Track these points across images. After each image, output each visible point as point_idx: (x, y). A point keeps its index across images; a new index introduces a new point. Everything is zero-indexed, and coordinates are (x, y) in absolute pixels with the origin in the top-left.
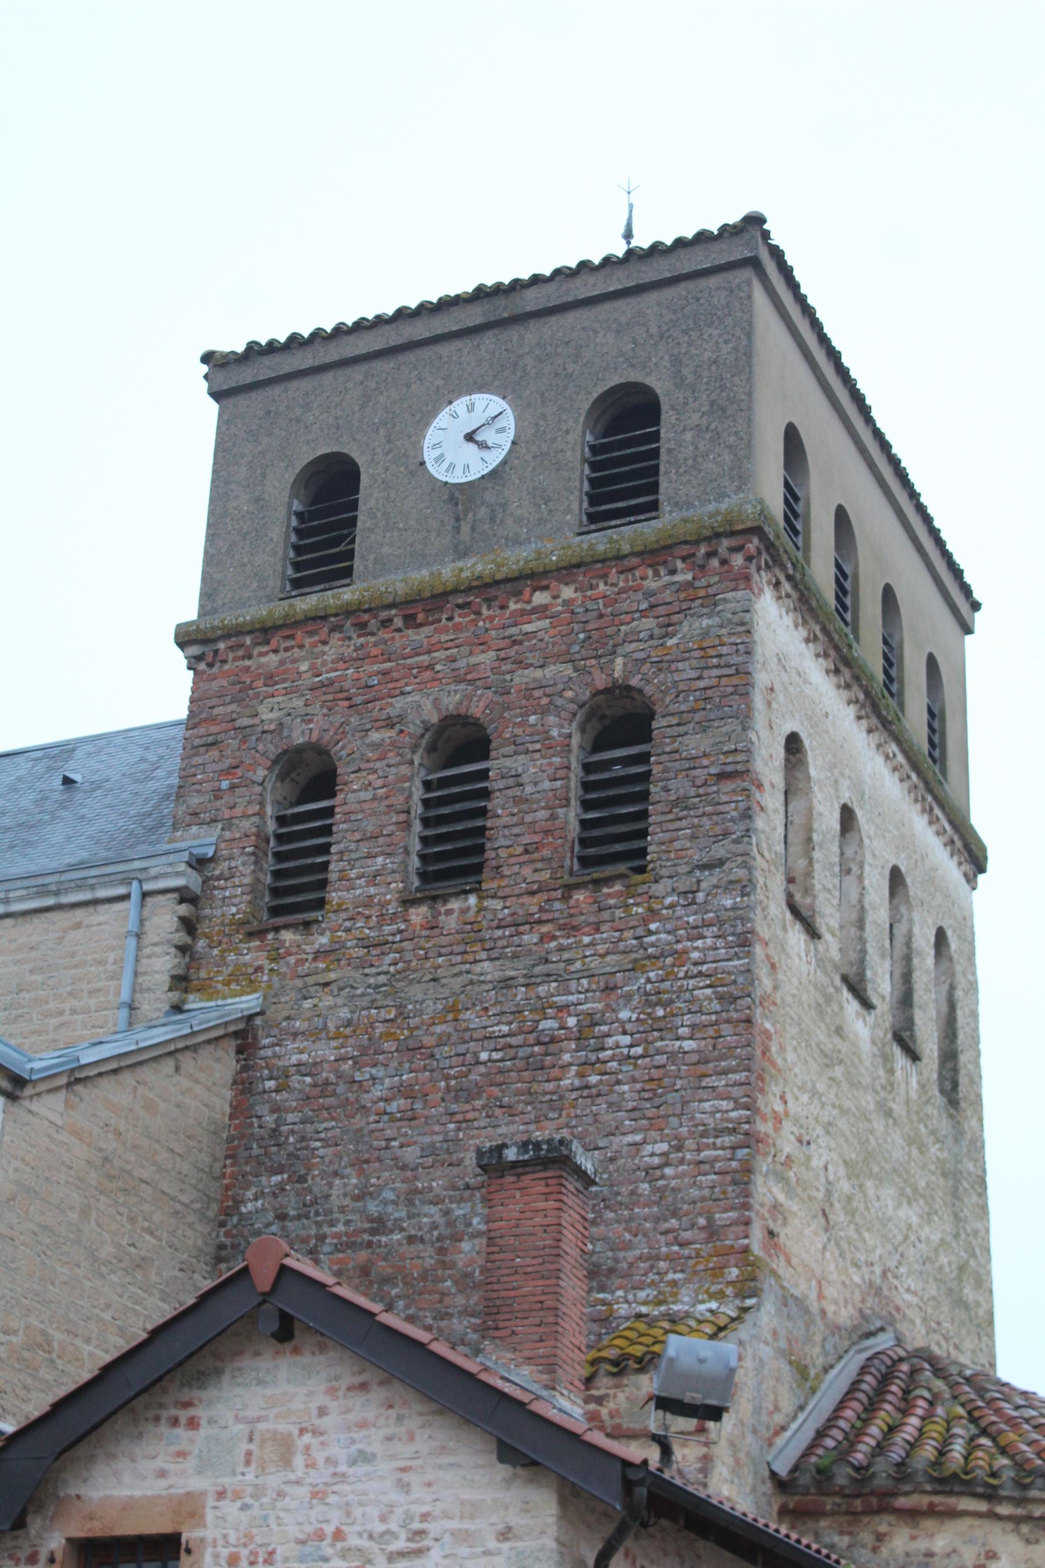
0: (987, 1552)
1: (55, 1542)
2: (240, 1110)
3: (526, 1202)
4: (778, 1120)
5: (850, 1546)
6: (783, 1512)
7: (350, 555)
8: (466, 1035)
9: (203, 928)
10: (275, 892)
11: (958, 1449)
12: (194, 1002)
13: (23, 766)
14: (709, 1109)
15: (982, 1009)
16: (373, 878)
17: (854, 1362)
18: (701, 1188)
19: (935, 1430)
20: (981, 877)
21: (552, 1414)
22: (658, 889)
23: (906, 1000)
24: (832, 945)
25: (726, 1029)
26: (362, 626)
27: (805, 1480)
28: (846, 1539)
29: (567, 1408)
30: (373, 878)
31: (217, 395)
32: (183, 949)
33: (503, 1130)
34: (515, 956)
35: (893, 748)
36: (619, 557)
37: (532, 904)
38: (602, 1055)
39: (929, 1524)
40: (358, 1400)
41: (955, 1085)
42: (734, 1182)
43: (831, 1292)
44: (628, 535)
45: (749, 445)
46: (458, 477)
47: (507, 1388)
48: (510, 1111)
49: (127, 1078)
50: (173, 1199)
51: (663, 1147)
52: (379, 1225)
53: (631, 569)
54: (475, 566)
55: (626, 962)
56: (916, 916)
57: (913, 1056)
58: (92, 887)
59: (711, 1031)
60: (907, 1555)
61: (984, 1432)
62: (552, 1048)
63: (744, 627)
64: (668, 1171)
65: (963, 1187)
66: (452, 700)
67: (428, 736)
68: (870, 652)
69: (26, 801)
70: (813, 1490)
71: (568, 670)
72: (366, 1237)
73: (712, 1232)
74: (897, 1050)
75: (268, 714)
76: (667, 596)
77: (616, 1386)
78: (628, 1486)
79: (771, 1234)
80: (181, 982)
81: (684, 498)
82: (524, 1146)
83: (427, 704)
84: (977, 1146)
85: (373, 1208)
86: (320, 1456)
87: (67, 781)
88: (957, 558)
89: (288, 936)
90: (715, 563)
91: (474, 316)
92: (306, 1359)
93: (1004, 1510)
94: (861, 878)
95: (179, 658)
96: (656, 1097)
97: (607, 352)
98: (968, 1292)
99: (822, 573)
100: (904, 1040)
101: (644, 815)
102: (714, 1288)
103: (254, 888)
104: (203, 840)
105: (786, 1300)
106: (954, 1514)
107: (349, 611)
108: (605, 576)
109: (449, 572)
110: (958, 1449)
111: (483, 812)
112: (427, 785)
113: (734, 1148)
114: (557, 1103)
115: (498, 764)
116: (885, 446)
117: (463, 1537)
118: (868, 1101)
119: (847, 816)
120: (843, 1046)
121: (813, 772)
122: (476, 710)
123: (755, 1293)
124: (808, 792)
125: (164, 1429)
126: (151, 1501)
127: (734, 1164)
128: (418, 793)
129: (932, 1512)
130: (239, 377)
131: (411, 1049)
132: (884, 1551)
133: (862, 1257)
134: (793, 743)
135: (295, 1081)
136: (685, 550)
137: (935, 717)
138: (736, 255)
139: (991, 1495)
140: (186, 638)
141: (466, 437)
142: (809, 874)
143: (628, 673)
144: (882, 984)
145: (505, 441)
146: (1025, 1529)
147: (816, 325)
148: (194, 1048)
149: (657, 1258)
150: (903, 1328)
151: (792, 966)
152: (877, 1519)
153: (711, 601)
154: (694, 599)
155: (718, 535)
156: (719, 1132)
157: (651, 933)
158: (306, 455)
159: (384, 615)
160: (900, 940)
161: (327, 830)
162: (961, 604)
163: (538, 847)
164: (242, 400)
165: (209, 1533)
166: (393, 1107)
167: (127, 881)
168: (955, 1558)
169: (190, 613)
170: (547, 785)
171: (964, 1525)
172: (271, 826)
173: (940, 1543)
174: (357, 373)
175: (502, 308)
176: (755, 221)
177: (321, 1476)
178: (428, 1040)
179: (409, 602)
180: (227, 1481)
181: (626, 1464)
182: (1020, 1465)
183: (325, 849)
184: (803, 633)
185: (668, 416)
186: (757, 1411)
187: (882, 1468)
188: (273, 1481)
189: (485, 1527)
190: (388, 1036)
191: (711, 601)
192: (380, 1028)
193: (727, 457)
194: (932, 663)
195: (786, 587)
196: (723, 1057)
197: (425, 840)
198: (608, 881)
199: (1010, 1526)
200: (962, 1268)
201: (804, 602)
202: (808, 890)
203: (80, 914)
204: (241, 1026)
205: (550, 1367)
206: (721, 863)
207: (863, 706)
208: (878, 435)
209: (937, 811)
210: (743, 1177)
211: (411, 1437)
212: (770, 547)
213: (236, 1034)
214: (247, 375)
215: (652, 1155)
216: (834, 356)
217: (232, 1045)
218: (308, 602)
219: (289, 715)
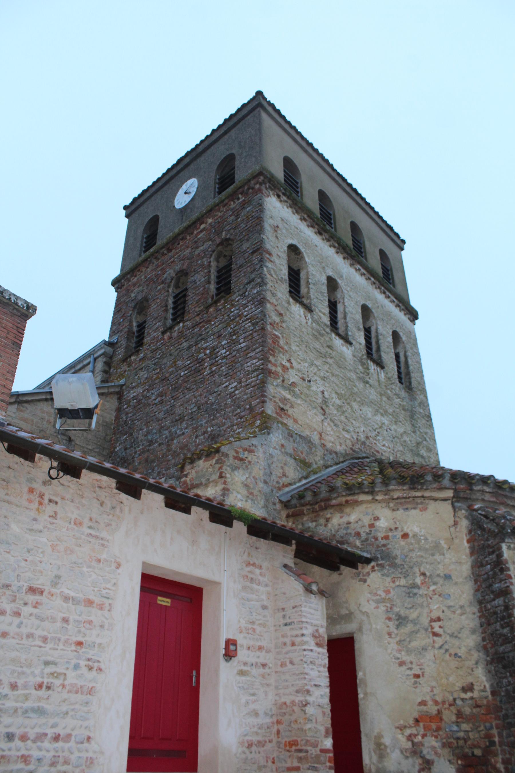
0: (374, 518)
5: (316, 526)
14: (249, 365)
18: (247, 394)
20: (416, 321)
22: (234, 297)
28: (314, 523)
33: (187, 397)
34: (193, 337)
35: (358, 266)
38: (217, 359)
39: (348, 510)
42: (258, 388)
48: (189, 389)
50: (83, 447)
51: (235, 384)
52: (151, 442)
53: (227, 204)
56: (378, 322)
57: (380, 364)
58: (82, 361)
59: (250, 337)
60: (339, 525)
62: (202, 363)
64: (237, 392)
67: (173, 282)
70: (298, 505)
71: (210, 243)
72: (147, 448)
77: (192, 468)
84: (425, 405)
85: (150, 437)
88: (389, 222)
90: (251, 190)
93: (379, 497)
94: (344, 303)
95: (113, 289)
102: (252, 431)
106: (357, 503)
108: (219, 210)
113: (257, 376)
121: (307, 260)
127: (258, 382)
132: (329, 525)
136: (241, 190)
140: (115, 283)
142: (308, 292)
146: (391, 505)
149: (233, 425)
152: (326, 512)
157: (232, 312)
159: (161, 251)
162: (400, 244)
166: (157, 401)
168: (360, 523)
170: (203, 279)
171: (362, 508)
173: (353, 518)
175: (194, 154)
178: (167, 375)
179: (167, 244)
190: (158, 378)
192: (155, 377)
196: (254, 344)
199: (384, 505)
204: (117, 390)
207: (338, 248)
209: (387, 293)
210: (262, 386)
213: (117, 393)
215: (232, 388)
217: (116, 397)
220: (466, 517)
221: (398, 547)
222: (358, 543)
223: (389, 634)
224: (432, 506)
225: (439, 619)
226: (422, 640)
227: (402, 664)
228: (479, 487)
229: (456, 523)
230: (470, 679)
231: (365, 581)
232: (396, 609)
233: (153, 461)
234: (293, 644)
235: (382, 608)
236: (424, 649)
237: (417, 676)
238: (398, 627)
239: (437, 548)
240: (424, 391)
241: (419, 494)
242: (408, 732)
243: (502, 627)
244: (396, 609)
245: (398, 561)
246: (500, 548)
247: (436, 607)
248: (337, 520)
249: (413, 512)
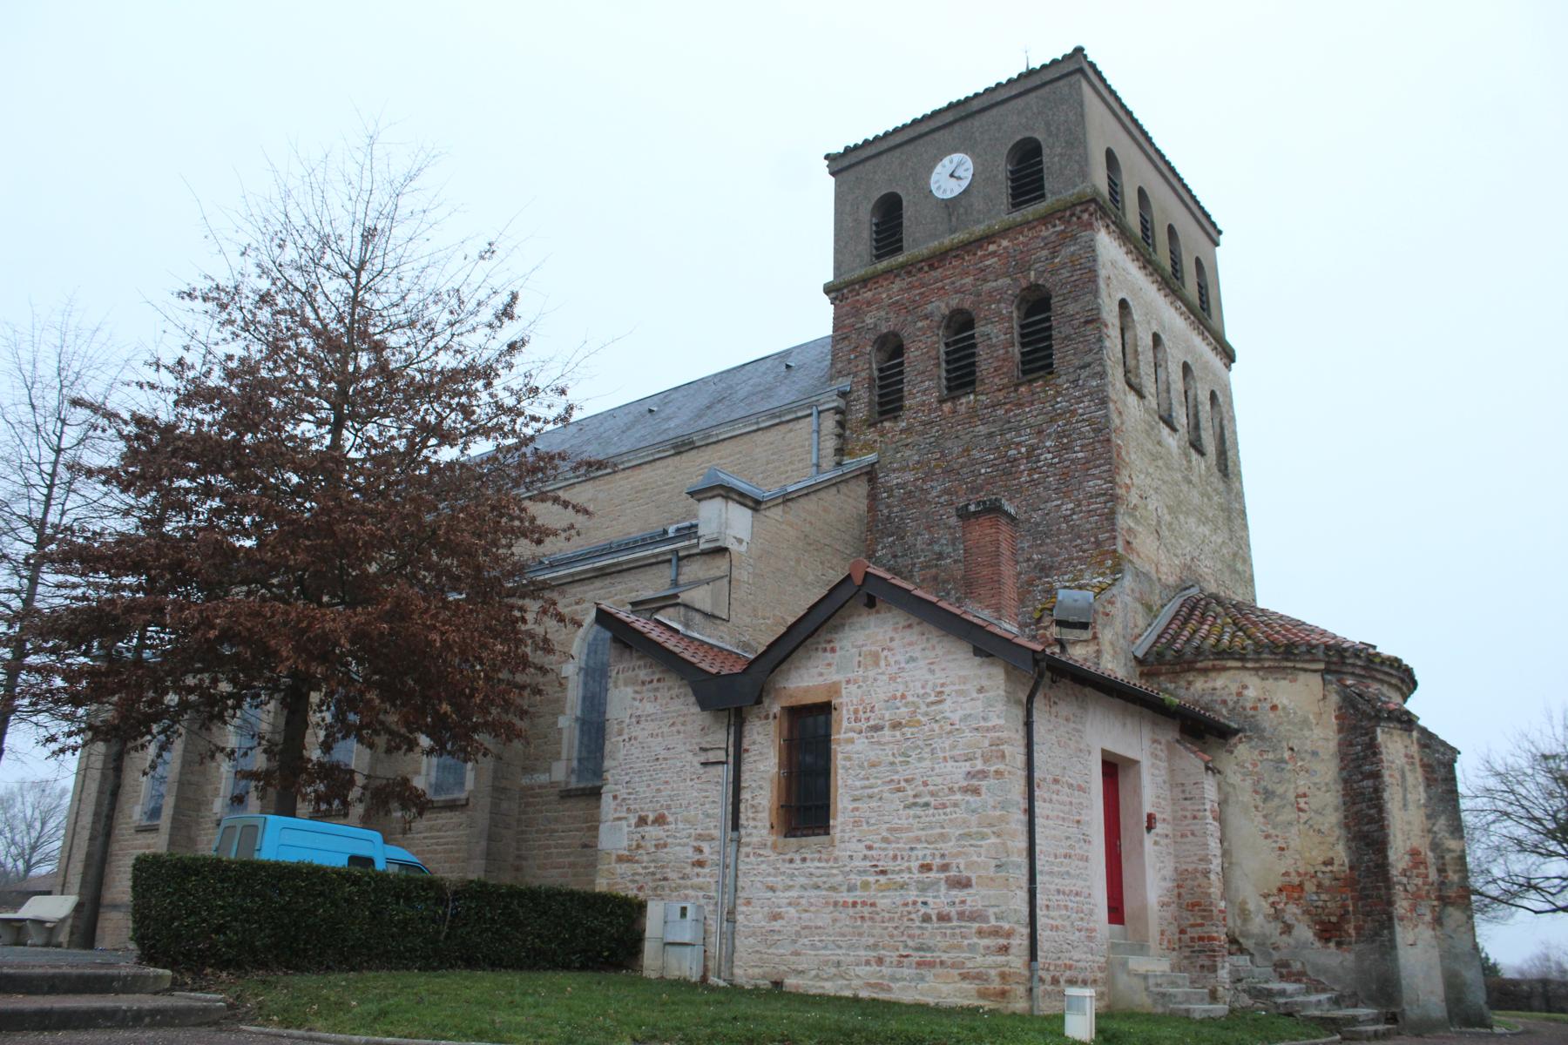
1: (776, 709)
2: (872, 508)
3: (981, 532)
4: (1128, 487)
6: (1142, 675)
7: (901, 240)
8: (974, 462)
9: (848, 425)
10: (881, 404)
11: (1226, 637)
12: (847, 460)
13: (769, 363)
14: (1092, 485)
15: (1238, 429)
16: (924, 392)
17: (1177, 602)
19: (1216, 630)
21: (997, 631)
22: (1059, 381)
23: (1196, 427)
24: (1152, 402)
25: (1098, 445)
26: (909, 273)
27: (1151, 659)
29: (1008, 627)
30: (924, 392)
31: (833, 174)
32: (839, 436)
35: (1179, 303)
36: (1028, 222)
37: (1001, 396)
39: (1213, 675)
40: (908, 632)
41: (1226, 466)
43: (1164, 569)
44: (1030, 211)
45: (1086, 160)
46: (948, 196)
47: (975, 620)
49: (813, 497)
52: (940, 556)
54: (961, 236)
55: (1047, 418)
57: (1201, 453)
61: (1240, 629)
63: (1091, 248)
65: (1233, 515)
66: (954, 302)
68: (1163, 257)
69: (770, 378)
71: (1008, 281)
73: (1098, 544)
74: (1192, 451)
75: (869, 321)
76: (1053, 238)
78: (1036, 662)
79: (1128, 543)
80: (840, 451)
81: (1057, 190)
82: (978, 504)
83: (943, 306)
84: (1240, 496)
85: (936, 548)
86: (892, 661)
87: (788, 367)
89: (887, 424)
91: (949, 117)
92: (882, 615)
93: (1249, 665)
95: (826, 299)
96: (1067, 481)
97: (1013, 125)
98: (1239, 566)
99: (1133, 219)
100: (1196, 445)
101: (1051, 346)
103: (870, 403)
104: (844, 383)
105: (1138, 574)
106: (1225, 669)
107: (902, 266)
109: (947, 241)
110: (1226, 637)
111: (973, 355)
112: (947, 345)
114: (1020, 489)
115: (979, 330)
116: (1162, 157)
117: (960, 693)
118: (1178, 476)
119: (1157, 340)
120: (1163, 451)
122: (967, 305)
123: (1120, 571)
124: (1134, 328)
125: (820, 653)
126: (816, 687)
128: (943, 349)
129: (1214, 669)
130: (844, 164)
131: (947, 472)
133: (1179, 552)
134: (1123, 304)
135: (896, 492)
137: (1203, 289)
138: (1071, 68)
139: (1243, 658)
140: (828, 289)
141: (950, 176)
142: (1137, 367)
143: (1037, 278)
144: (1181, 418)
145: (969, 175)
147: (1118, 99)
148: (846, 481)
150: (1204, 585)
151: (1130, 412)
153: (1074, 238)
154: (1065, 238)
155: (1074, 205)
156: (1098, 495)
158: (876, 195)
160: (1190, 399)
161: (901, 373)
162: (1212, 233)
163: (1001, 367)
164: (845, 174)
165: (844, 700)
167: (810, 407)
169: (829, 277)
172: (876, 373)
174: (897, 153)
175: (962, 112)
176: (1079, 51)
177: (893, 669)
179: (929, 258)
180: (850, 675)
181: (1034, 652)
182: (1257, 643)
183: (901, 382)
184: (1124, 249)
185: (1046, 151)
186: (1125, 627)
187: (1188, 649)
188: (871, 674)
189: (971, 687)
190: (937, 466)
191: (1074, 238)
193: (1076, 167)
194: (1198, 262)
195: (1113, 227)
197: (948, 371)
198: (1035, 380)
200: (1235, 555)
201: (1124, 235)
202: (1138, 375)
203: (791, 425)
205: (998, 609)
206: (1089, 365)
208: (1158, 151)
210: (1111, 516)
211: (934, 648)
212: (1101, 208)
214: (845, 162)
216: (1129, 114)
217: (865, 478)
218: (883, 265)
219: (878, 320)
220: (1338, 693)
221: (1267, 720)
222: (1224, 712)
223: (1256, 807)
224: (1302, 677)
225: (1305, 795)
226: (1288, 815)
227: (1267, 837)
228: (1350, 661)
229: (1325, 697)
230: (1331, 854)
231: (1232, 752)
232: (1263, 783)
233: (946, 582)
234: (1195, 818)
235: (1249, 782)
236: (1290, 824)
237: (1282, 849)
238: (1265, 801)
239: (1305, 722)
240: (1239, 475)
241: (1290, 664)
242: (1271, 899)
243: (1369, 808)
244: (1263, 783)
245: (1266, 734)
246: (1374, 732)
247: (1303, 783)
248: (1200, 684)
249: (1283, 683)
